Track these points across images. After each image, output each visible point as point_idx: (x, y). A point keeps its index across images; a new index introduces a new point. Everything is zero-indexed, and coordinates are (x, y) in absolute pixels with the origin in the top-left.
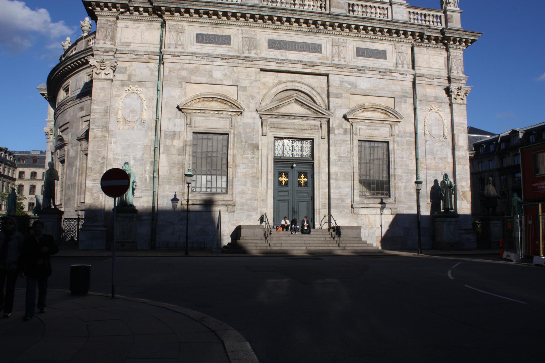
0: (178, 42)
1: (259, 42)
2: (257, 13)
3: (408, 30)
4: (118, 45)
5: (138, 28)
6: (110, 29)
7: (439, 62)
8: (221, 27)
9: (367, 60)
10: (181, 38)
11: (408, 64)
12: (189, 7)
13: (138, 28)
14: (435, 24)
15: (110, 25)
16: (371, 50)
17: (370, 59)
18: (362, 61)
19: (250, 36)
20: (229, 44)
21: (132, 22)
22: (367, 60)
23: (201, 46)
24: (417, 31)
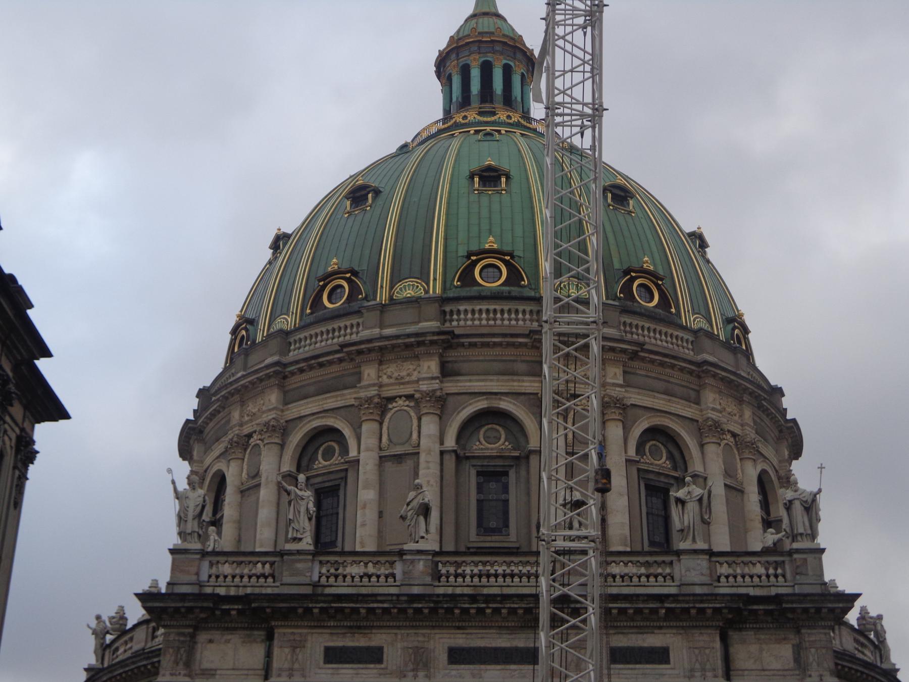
0: (293, 664)
1: (432, 654)
2: (426, 605)
3: (706, 605)
4: (196, 674)
5: (228, 641)
6: (183, 649)
7: (782, 656)
8: (366, 631)
9: (632, 669)
10: (300, 657)
11: (714, 670)
12: (310, 605)
13: (229, 642)
14: (772, 579)
15: (183, 642)
16: (641, 649)
17: (638, 666)
18: (621, 672)
19: (416, 644)
20: (380, 661)
21: (219, 632)
22: (632, 669)
23: (333, 668)
24: (723, 605)
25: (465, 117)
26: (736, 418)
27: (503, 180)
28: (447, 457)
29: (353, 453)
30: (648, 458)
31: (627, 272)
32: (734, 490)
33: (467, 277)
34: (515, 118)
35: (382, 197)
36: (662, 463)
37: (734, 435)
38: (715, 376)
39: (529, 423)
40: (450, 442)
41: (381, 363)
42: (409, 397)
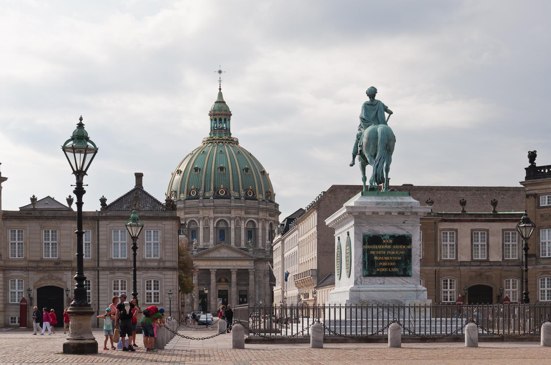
25: (216, 138)
26: (265, 216)
27: (224, 169)
28: (215, 228)
29: (198, 226)
30: (248, 226)
31: (247, 190)
32: (264, 229)
33: (218, 193)
34: (227, 138)
35: (201, 170)
36: (251, 226)
37: (264, 219)
38: (261, 210)
39: (228, 222)
40: (215, 225)
41: (203, 210)
42: (208, 217)
